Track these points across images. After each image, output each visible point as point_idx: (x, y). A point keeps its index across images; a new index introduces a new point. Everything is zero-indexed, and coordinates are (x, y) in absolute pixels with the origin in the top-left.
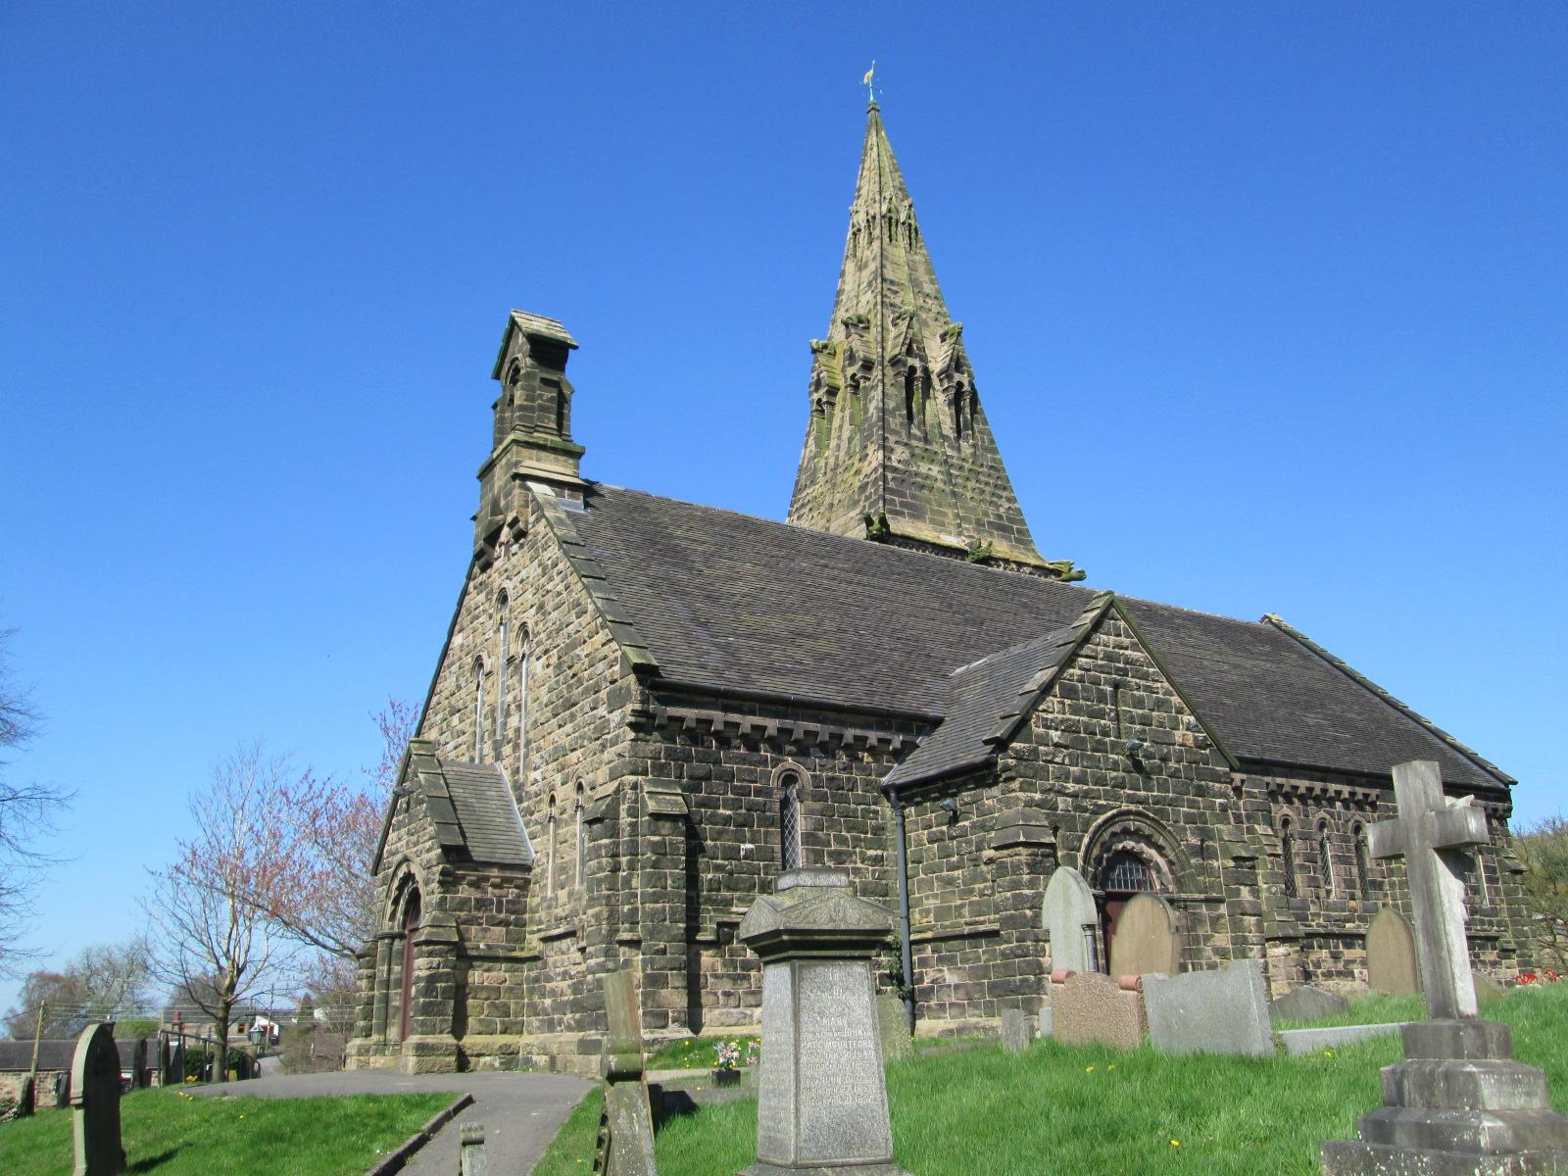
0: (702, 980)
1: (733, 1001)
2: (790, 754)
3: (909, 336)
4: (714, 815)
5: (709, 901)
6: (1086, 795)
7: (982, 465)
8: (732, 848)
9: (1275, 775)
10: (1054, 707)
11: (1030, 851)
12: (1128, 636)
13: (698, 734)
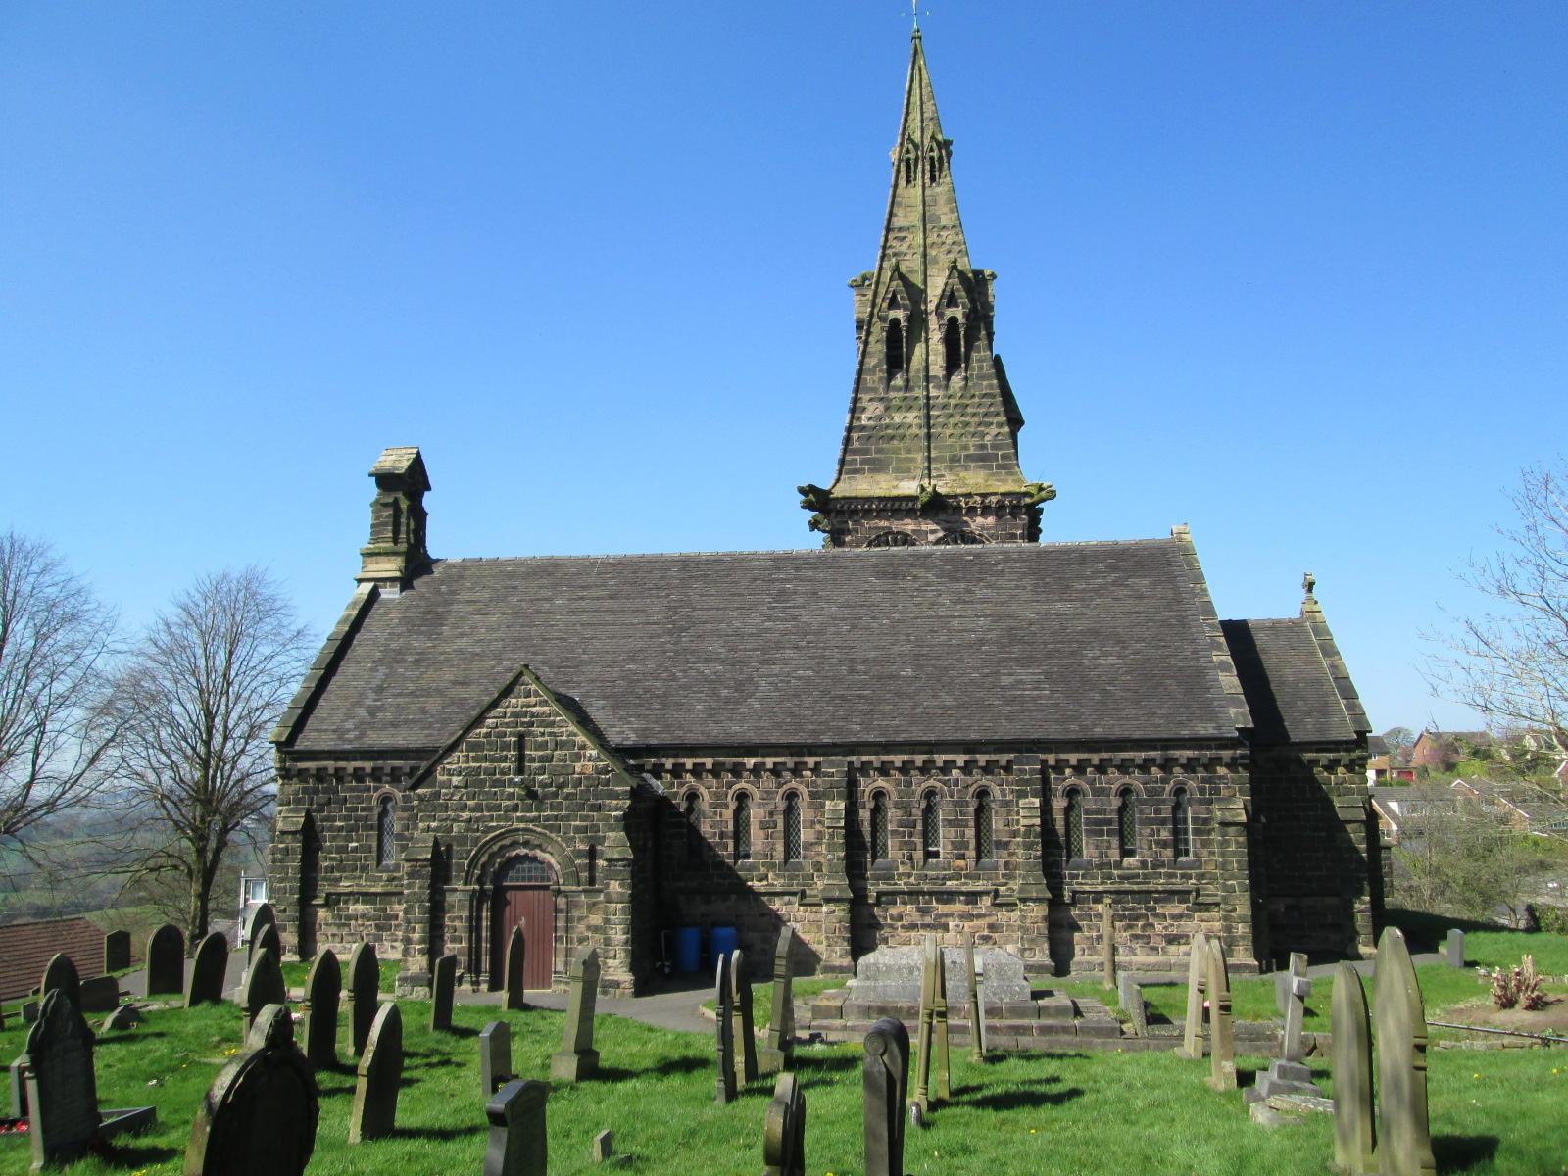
0: (317, 927)
1: (338, 939)
2: (387, 782)
3: (891, 289)
4: (332, 826)
5: (325, 879)
6: (478, 820)
7: (973, 396)
8: (342, 846)
9: (860, 753)
10: (456, 761)
11: (410, 864)
12: (537, 694)
13: (320, 776)
